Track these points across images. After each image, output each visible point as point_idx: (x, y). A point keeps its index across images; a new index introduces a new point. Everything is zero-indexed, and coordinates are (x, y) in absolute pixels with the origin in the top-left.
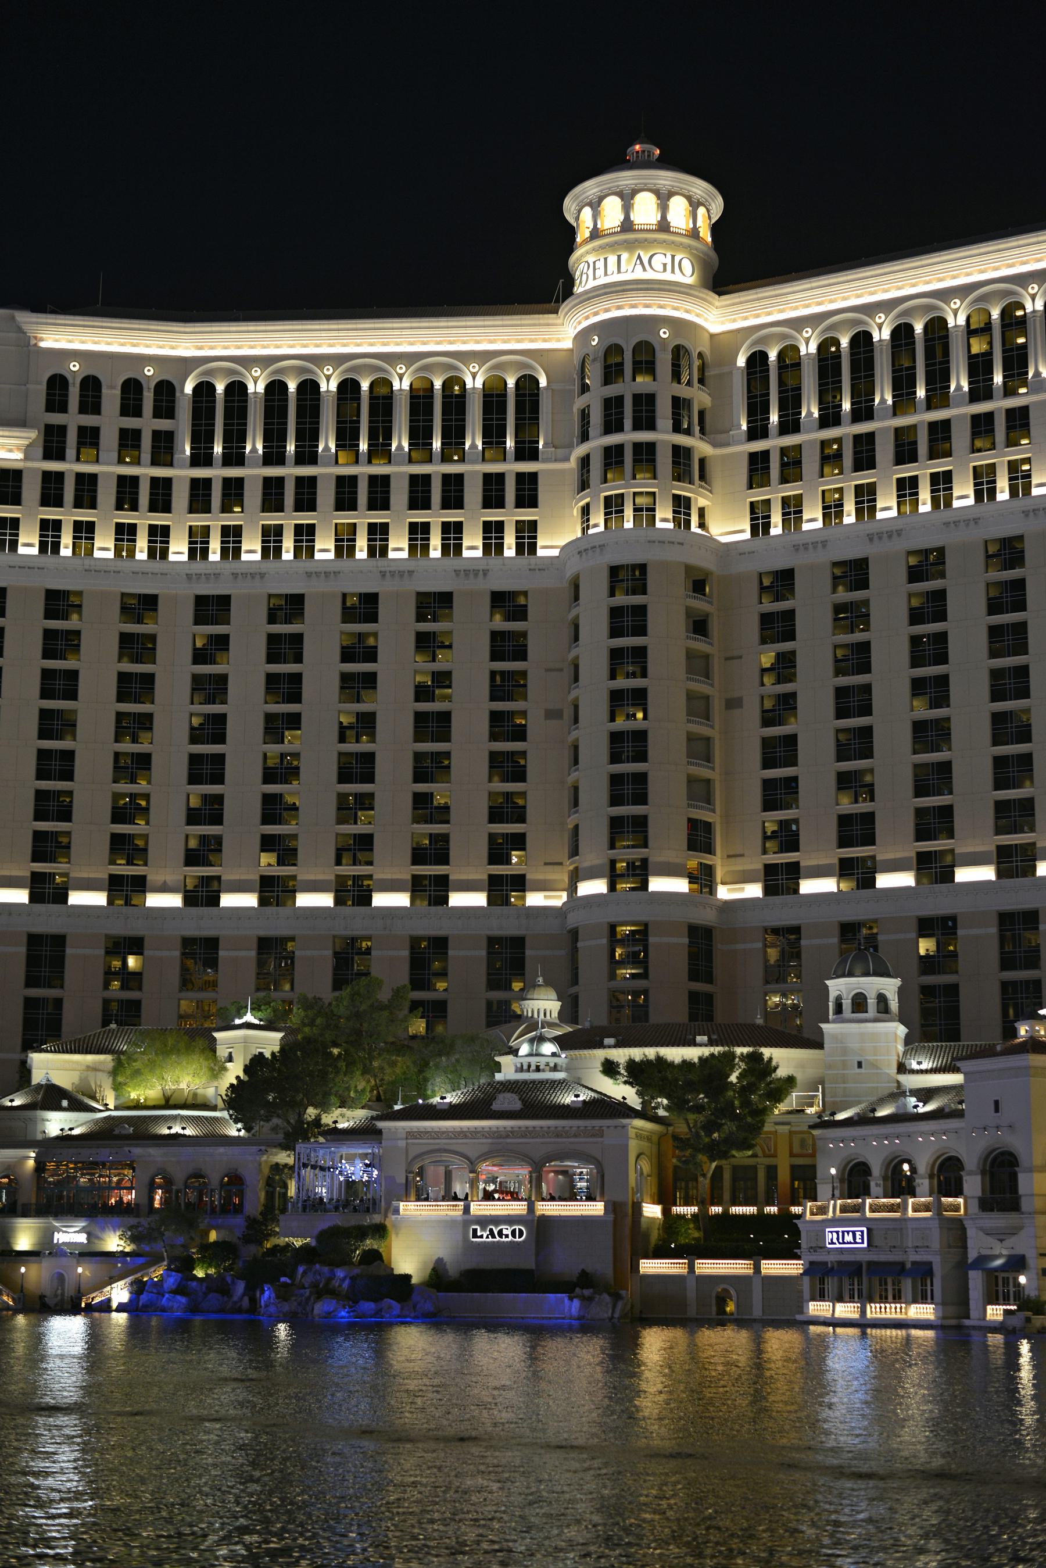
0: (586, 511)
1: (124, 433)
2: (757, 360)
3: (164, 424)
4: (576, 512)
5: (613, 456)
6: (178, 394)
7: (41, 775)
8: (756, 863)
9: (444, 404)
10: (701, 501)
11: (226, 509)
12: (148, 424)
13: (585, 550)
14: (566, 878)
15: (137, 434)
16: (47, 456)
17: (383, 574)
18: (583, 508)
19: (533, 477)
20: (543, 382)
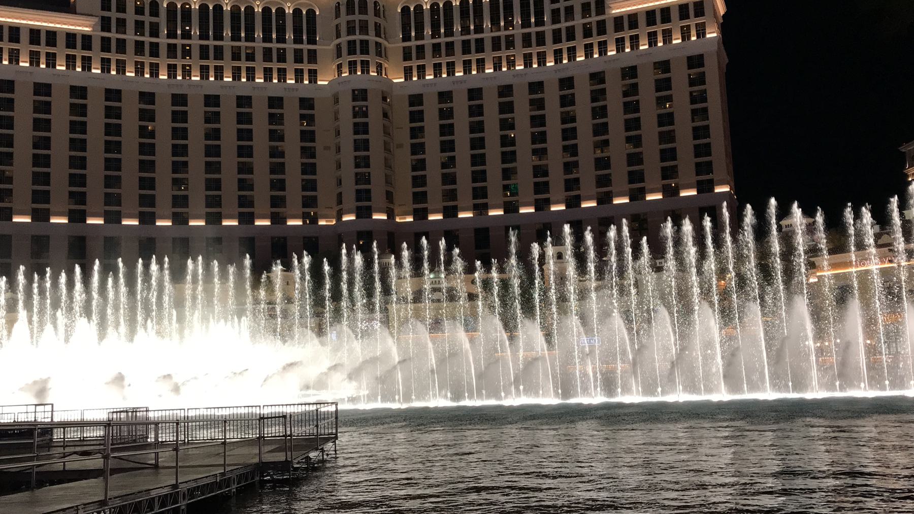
0: (339, 67)
1: (137, 22)
2: (405, 10)
3: (154, 19)
4: (334, 67)
5: (351, 45)
6: (160, 6)
7: (107, 168)
8: (441, 205)
9: (307, 20)
10: (385, 65)
11: (184, 57)
12: (147, 19)
13: (342, 82)
14: (335, 213)
15: (143, 22)
16: (103, 30)
17: (254, 88)
18: (338, 65)
19: (315, 51)
20: (317, 13)
